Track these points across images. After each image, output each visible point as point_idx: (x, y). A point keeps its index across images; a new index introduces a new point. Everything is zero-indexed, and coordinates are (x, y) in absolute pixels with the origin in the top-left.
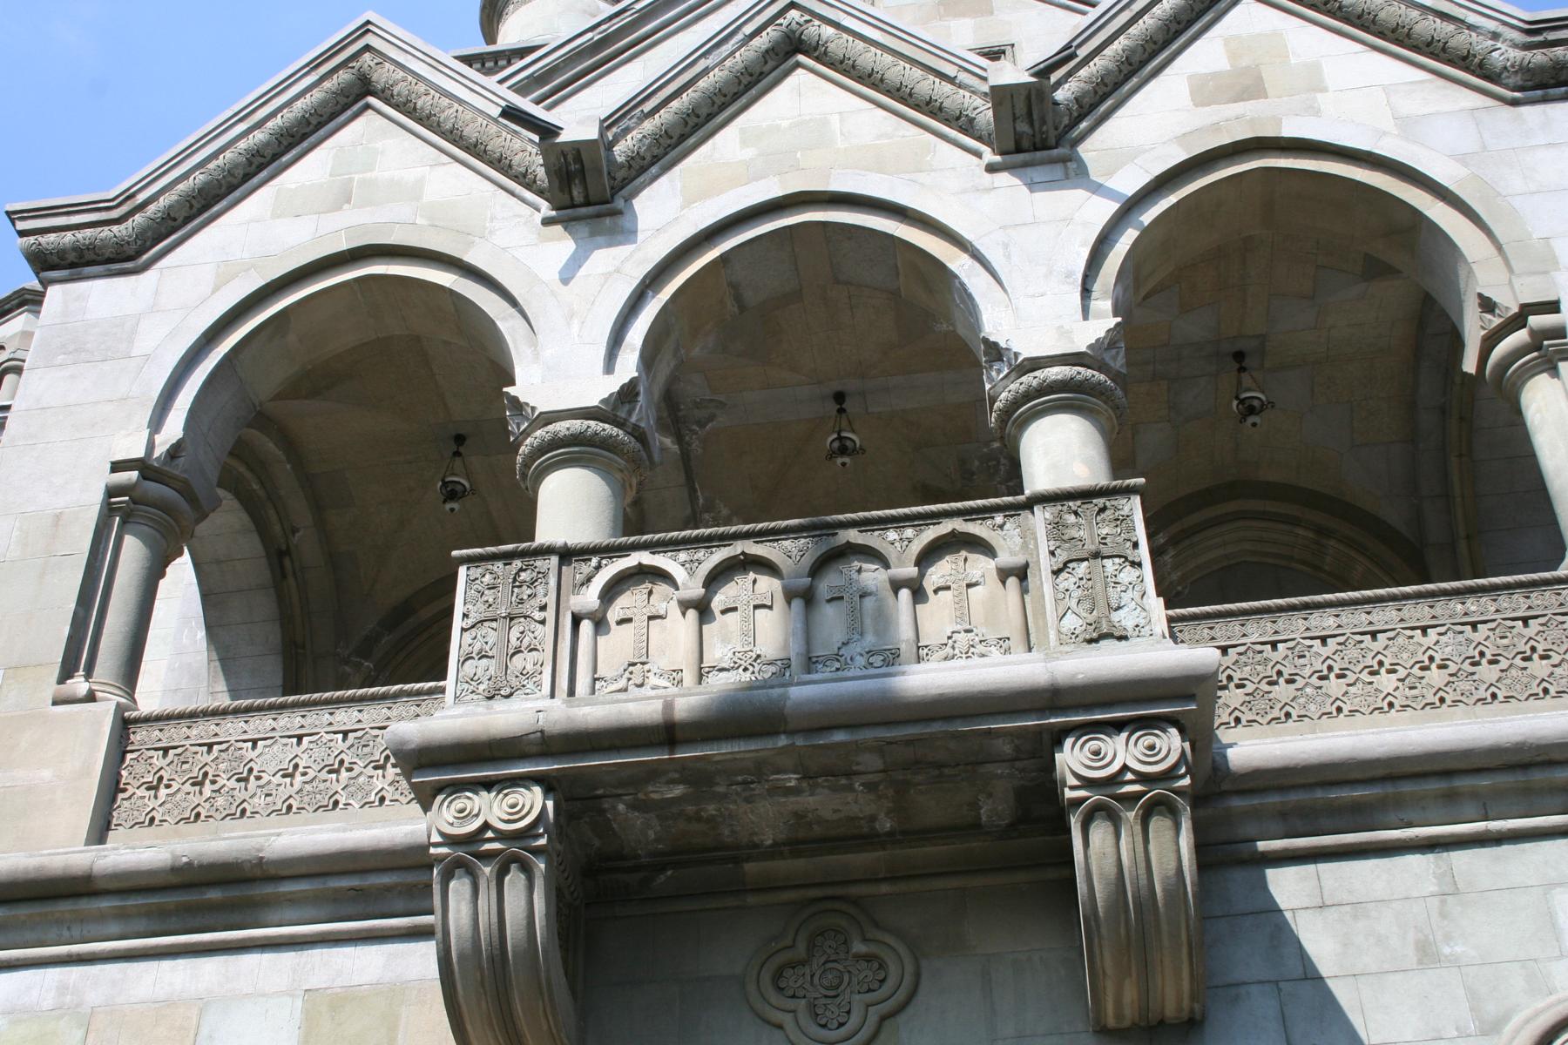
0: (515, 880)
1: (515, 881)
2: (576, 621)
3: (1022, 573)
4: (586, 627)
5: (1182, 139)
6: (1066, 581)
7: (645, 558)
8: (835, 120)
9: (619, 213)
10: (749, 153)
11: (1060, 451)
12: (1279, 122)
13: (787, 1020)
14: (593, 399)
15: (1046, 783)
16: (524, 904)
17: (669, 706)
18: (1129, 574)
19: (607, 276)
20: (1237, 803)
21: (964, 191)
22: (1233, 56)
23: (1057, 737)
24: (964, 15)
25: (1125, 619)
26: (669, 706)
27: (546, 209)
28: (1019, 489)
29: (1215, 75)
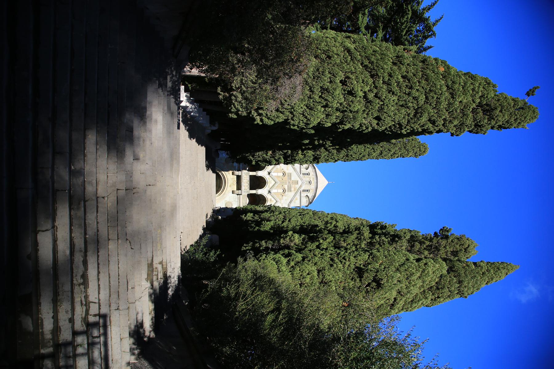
11: (253, 192)
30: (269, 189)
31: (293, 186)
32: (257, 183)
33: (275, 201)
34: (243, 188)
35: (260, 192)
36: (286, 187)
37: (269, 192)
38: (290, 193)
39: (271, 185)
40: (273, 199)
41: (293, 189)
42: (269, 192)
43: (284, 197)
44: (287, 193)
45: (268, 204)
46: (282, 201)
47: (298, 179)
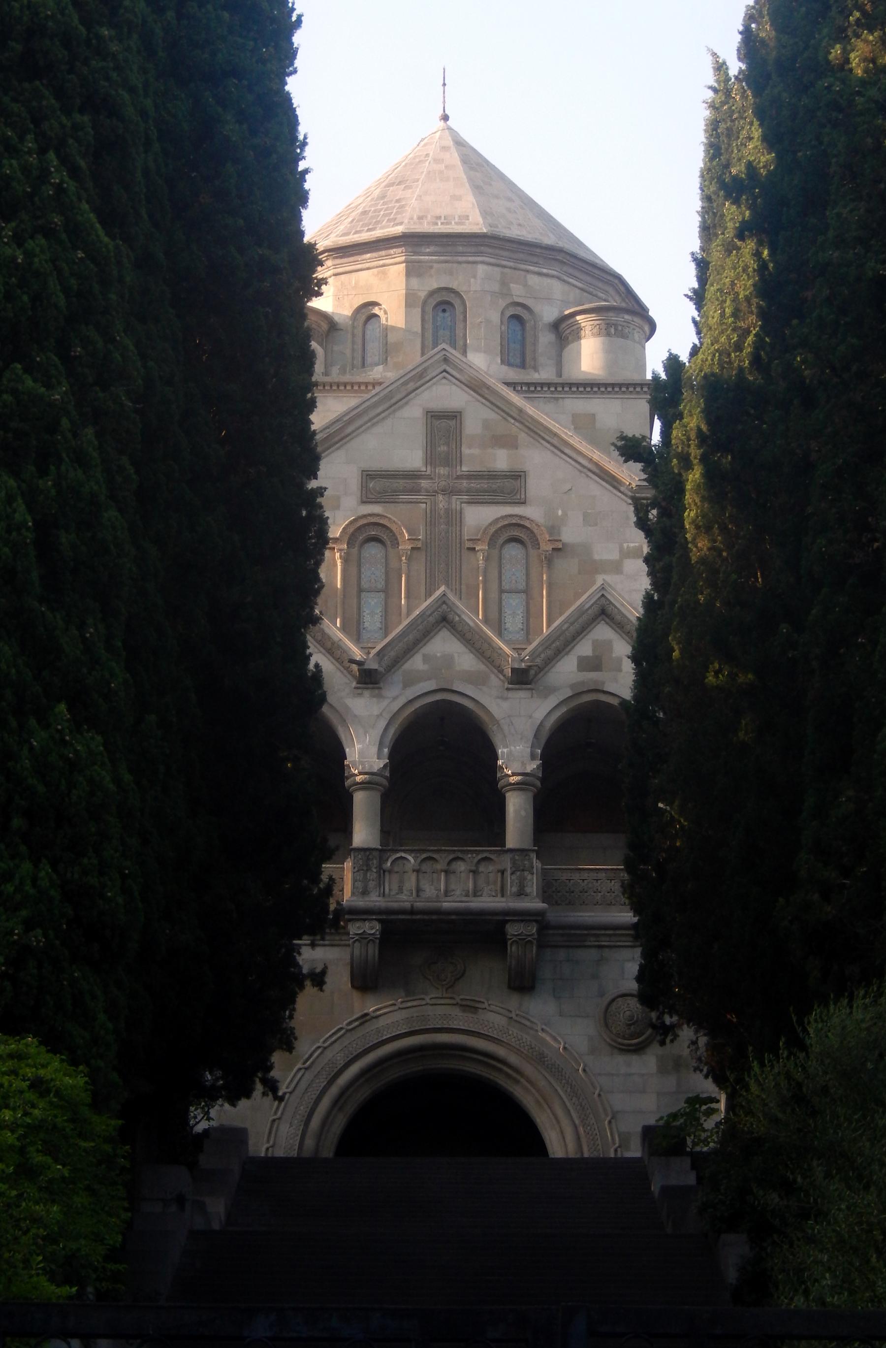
0: (370, 946)
1: (370, 946)
2: (384, 871)
3: (503, 872)
4: (387, 874)
5: (572, 686)
6: (514, 877)
7: (403, 855)
8: (456, 655)
9: (380, 688)
10: (425, 667)
12: (603, 683)
13: (431, 978)
14: (375, 769)
15: (503, 933)
16: (373, 951)
17: (412, 906)
18: (529, 877)
19: (378, 716)
20: (551, 932)
21: (498, 697)
22: (593, 650)
23: (507, 921)
24: (502, 446)
25: (528, 890)
26: (412, 906)
27: (354, 684)
28: (503, 844)
29: (587, 657)
30: (495, 681)
31: (473, 457)
32: (442, 760)
33: (603, 632)
34: (489, 902)
35: (516, 757)
36: (479, 517)
37: (522, 678)
38: (535, 486)
39: (466, 660)
40: (584, 648)
41: (501, 460)
42: (522, 678)
43: (568, 535)
44: (532, 512)
45: (622, 682)
46: (605, 552)
47: (414, 411)
